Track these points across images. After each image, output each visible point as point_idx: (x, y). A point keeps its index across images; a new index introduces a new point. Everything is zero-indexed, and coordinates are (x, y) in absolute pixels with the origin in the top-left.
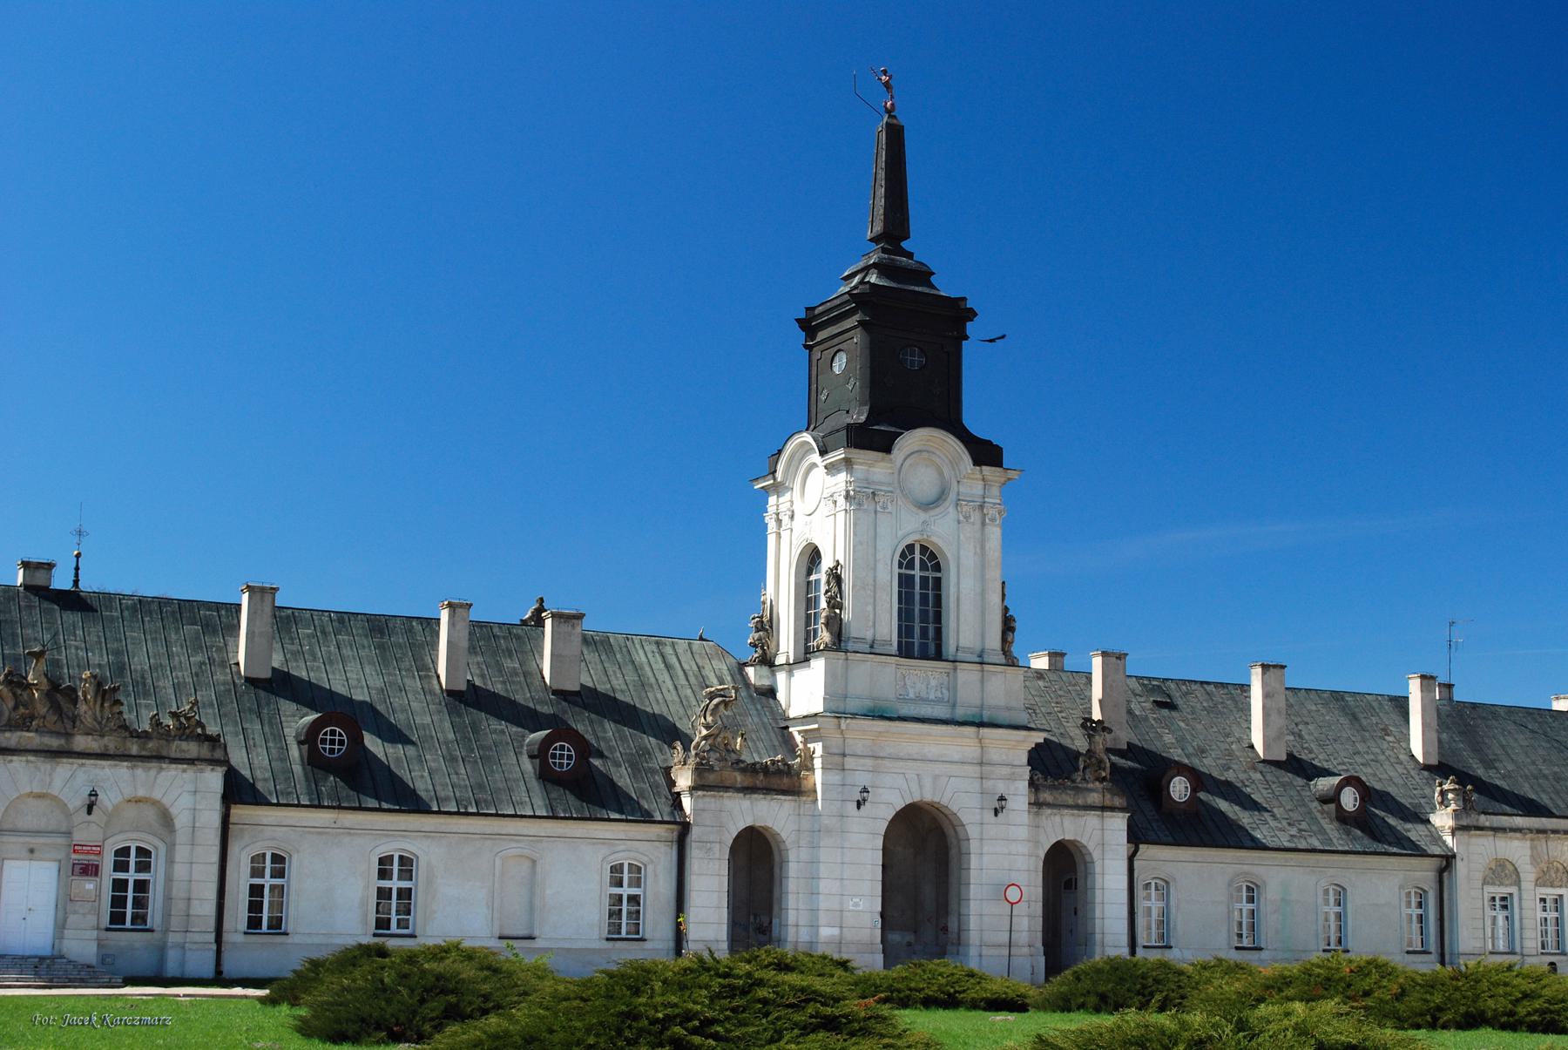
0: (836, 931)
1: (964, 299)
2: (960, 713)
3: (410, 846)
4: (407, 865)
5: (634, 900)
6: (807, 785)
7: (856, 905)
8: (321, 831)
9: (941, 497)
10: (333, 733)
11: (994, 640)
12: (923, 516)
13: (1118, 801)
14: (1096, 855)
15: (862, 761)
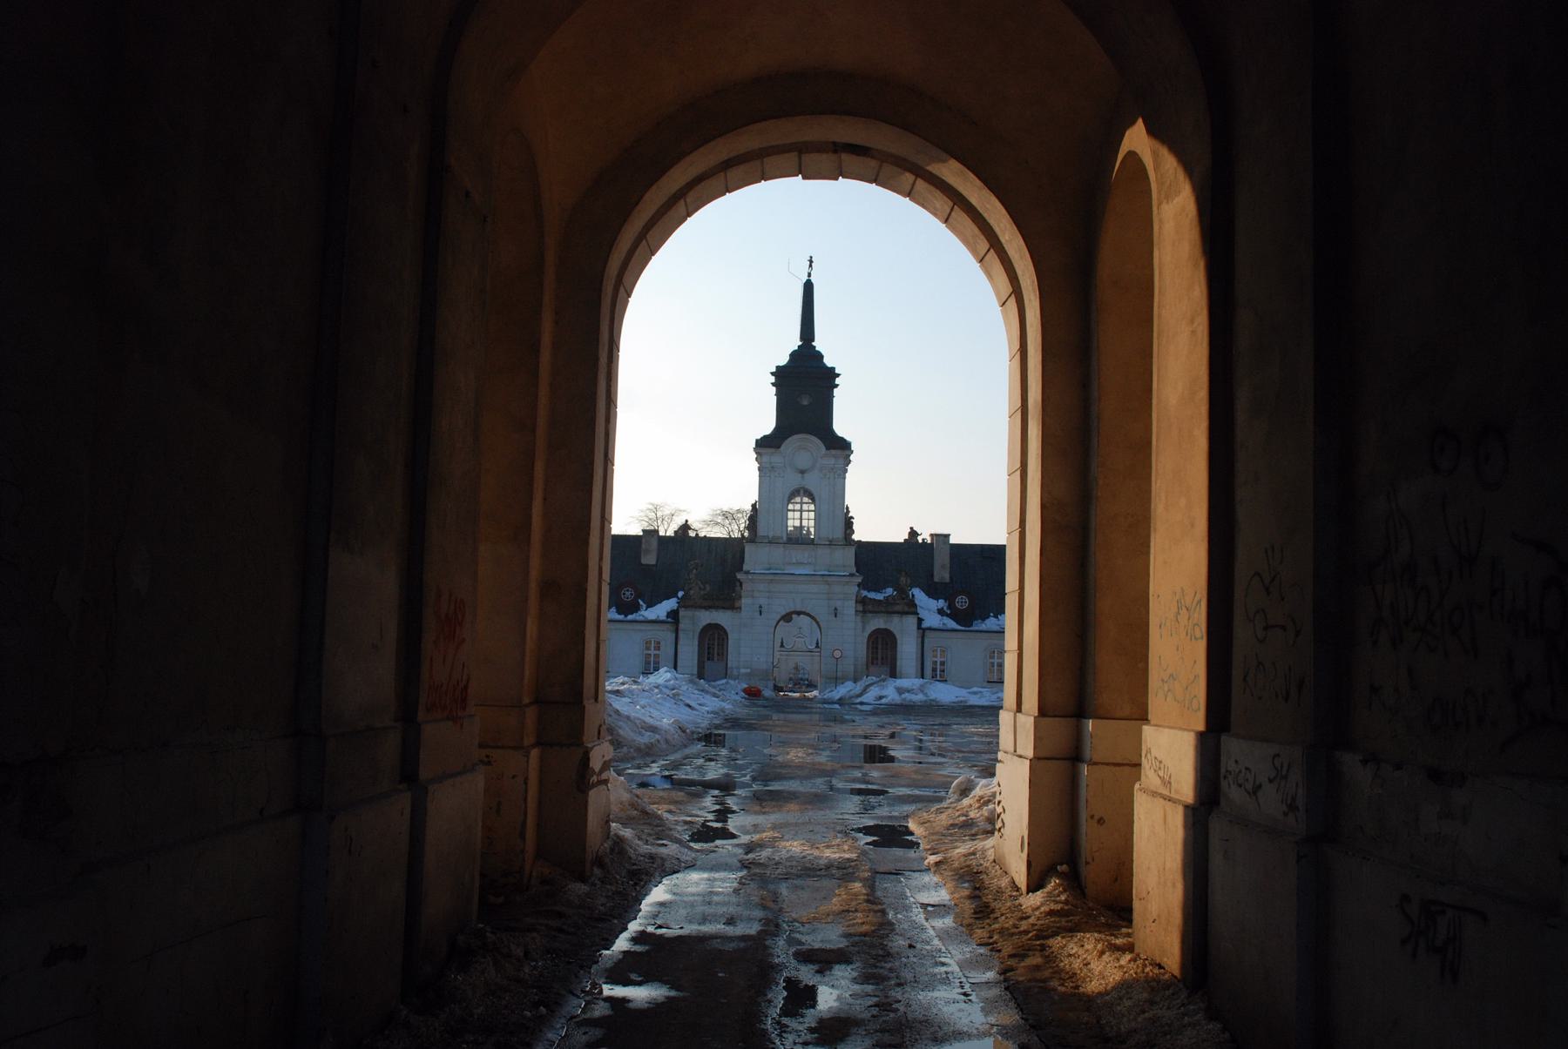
11: (839, 534)
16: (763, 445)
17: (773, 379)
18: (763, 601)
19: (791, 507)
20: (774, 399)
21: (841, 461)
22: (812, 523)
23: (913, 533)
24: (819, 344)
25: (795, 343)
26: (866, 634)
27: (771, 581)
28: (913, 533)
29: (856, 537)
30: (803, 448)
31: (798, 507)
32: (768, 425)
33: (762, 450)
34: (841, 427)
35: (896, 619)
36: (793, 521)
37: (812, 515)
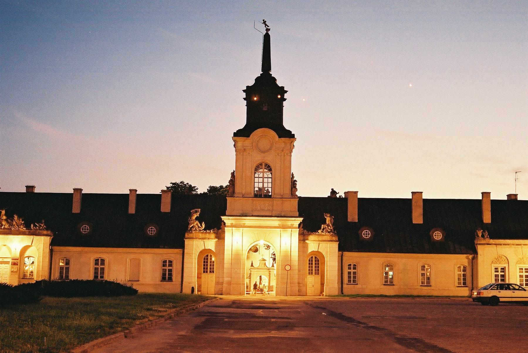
0: (230, 279)
1: (283, 88)
3: (104, 256)
4: (103, 261)
8: (80, 253)
9: (270, 149)
10: (85, 227)
12: (263, 155)
13: (334, 238)
16: (238, 134)
17: (244, 95)
20: (245, 108)
21: (288, 145)
22: (270, 185)
23: (333, 192)
24: (274, 73)
25: (258, 72)
29: (299, 193)
31: (261, 175)
32: (242, 123)
33: (236, 138)
34: (287, 124)
36: (258, 185)
37: (270, 180)
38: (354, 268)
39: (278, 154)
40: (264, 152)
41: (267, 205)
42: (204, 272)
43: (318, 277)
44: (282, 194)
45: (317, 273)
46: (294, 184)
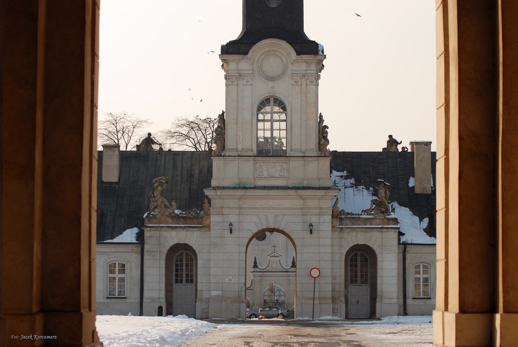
2: (290, 183)
5: (122, 280)
6: (206, 223)
7: (230, 280)
9: (283, 74)
12: (271, 84)
14: (377, 252)
15: (233, 210)
16: (229, 50)
18: (233, 219)
19: (261, 117)
21: (313, 67)
22: (283, 134)
23: (392, 142)
26: (344, 252)
27: (241, 197)
28: (392, 142)
29: (331, 147)
30: (274, 53)
31: (268, 117)
32: (234, 29)
33: (227, 57)
34: (311, 30)
35: (376, 234)
37: (283, 125)
38: (425, 272)
39: (296, 82)
40: (271, 79)
41: (279, 168)
42: (177, 281)
43: (366, 289)
44: (304, 149)
45: (364, 282)
46: (322, 132)
